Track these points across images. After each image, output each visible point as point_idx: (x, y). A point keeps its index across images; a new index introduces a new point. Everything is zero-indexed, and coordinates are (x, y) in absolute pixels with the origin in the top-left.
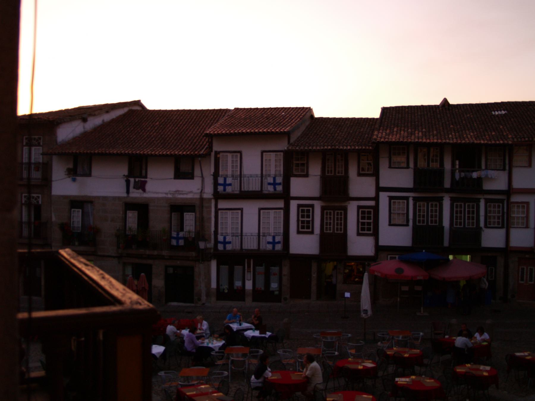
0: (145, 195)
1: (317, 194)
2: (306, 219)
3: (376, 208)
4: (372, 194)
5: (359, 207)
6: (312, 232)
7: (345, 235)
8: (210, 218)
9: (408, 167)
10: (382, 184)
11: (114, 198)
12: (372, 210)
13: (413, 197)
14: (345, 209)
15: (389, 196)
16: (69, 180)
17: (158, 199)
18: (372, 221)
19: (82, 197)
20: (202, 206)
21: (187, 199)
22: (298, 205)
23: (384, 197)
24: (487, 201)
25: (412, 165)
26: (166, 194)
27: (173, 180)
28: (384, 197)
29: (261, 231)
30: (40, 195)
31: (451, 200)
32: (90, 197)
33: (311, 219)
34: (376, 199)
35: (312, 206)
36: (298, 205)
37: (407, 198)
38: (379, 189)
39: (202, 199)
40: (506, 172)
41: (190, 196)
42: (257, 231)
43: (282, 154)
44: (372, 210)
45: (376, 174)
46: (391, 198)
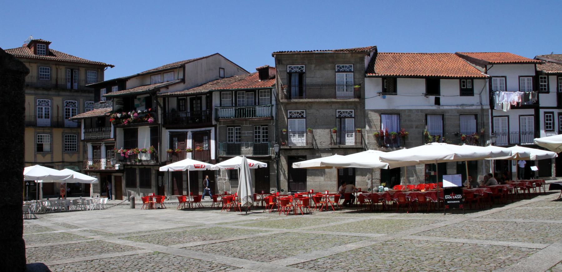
0: (441, 108)
1: (555, 105)
2: (549, 122)
8: (489, 123)
11: (417, 111)
16: (379, 99)
17: (452, 110)
19: (391, 110)
20: (482, 115)
21: (472, 110)
22: (544, 112)
26: (457, 106)
27: (459, 96)
29: (521, 131)
30: (353, 110)
32: (397, 110)
35: (553, 113)
36: (544, 112)
39: (482, 110)
41: (474, 107)
42: (519, 131)
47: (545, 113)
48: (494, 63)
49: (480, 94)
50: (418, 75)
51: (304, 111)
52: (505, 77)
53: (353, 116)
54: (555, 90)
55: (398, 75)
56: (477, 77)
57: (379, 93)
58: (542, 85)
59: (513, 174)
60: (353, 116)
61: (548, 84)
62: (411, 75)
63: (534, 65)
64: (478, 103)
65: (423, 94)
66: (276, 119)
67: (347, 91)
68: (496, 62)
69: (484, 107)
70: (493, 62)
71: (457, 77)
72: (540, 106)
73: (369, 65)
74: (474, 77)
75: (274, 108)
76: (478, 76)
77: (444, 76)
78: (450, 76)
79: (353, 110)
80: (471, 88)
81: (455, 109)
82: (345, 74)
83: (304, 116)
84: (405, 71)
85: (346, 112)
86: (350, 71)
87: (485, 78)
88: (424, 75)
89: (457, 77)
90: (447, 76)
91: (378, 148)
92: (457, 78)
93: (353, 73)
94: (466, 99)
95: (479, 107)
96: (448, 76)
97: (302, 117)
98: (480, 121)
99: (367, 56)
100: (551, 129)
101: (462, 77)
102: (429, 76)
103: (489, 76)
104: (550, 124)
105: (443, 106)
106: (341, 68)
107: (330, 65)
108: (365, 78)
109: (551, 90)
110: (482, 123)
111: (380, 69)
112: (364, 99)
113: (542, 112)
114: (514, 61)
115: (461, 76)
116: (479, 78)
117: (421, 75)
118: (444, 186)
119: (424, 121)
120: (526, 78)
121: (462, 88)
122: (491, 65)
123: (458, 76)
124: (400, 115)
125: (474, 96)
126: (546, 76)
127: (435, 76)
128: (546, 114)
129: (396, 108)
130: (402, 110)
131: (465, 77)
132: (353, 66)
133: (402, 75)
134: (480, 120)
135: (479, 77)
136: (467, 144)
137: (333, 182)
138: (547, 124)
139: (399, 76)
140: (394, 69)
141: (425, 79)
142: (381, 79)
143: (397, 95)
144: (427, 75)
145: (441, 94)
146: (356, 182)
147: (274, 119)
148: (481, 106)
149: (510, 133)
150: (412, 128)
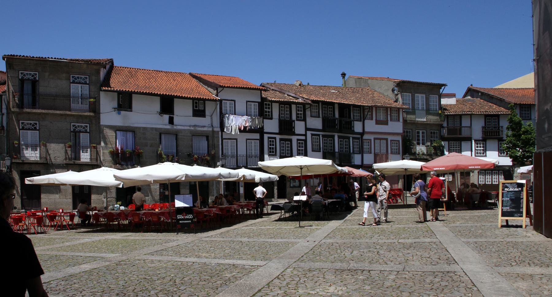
0: (175, 127)
1: (277, 131)
2: (272, 147)
3: (305, 141)
5: (298, 140)
8: (219, 145)
9: (319, 117)
10: (308, 127)
11: (152, 129)
12: (303, 142)
13: (322, 135)
14: (291, 140)
15: (311, 134)
16: (115, 114)
17: (184, 130)
19: (126, 127)
21: (204, 131)
24: (353, 138)
25: (321, 116)
26: (190, 126)
27: (192, 117)
28: (309, 133)
29: (248, 154)
30: (88, 125)
31: (338, 137)
34: (305, 135)
35: (275, 138)
37: (319, 135)
38: (307, 129)
39: (213, 131)
40: (362, 122)
41: (205, 129)
42: (246, 154)
43: (257, 104)
44: (303, 142)
45: (305, 120)
47: (269, 138)
48: (225, 86)
49: (211, 116)
50: (153, 93)
51: (37, 122)
52: (234, 101)
53: (88, 131)
54: (278, 117)
55: (133, 91)
56: (208, 99)
57: (115, 109)
58: (266, 112)
59: (241, 195)
60: (88, 131)
61: (272, 111)
62: (146, 92)
63: (260, 91)
64: (209, 125)
65: (157, 112)
66: (7, 129)
67: (82, 104)
68: (226, 86)
69: (215, 129)
70: (224, 85)
71: (190, 97)
72: (265, 131)
73: (105, 78)
74: (206, 98)
75: (5, 117)
76: (210, 98)
77: (178, 95)
78: (183, 96)
79: (88, 125)
80: (203, 109)
81: (187, 129)
82: (80, 85)
83: (38, 128)
84: (141, 87)
85: (81, 126)
86: (86, 83)
87: (215, 100)
88: (159, 93)
89: (190, 97)
90: (181, 96)
91: (113, 166)
92: (190, 98)
93: (88, 85)
94: (199, 121)
95: (210, 129)
96: (182, 96)
97: (35, 129)
98: (211, 143)
99: (103, 68)
100: (274, 154)
101: (195, 97)
102: (163, 94)
103: (219, 99)
104: (273, 148)
105: (176, 125)
106: (76, 79)
107: (64, 75)
108: (101, 92)
109: (274, 117)
110: (213, 144)
111: (116, 83)
112: (99, 113)
113: (266, 136)
114: (243, 87)
115: (194, 97)
116: (211, 100)
117: (156, 93)
118: (176, 206)
119: (158, 140)
120: (253, 104)
121: (195, 108)
122: (222, 88)
123: (191, 97)
124: (135, 132)
125: (205, 117)
126: (270, 103)
127: (169, 95)
128: (269, 140)
129: (132, 125)
130: (137, 128)
131: (198, 98)
132: (88, 78)
133: (137, 91)
134: (211, 141)
135: (211, 99)
136: (198, 165)
137: (68, 200)
138: (270, 148)
139: (135, 93)
140: (130, 85)
141: (159, 97)
142: (116, 94)
143: (132, 111)
144: (162, 93)
145: (175, 114)
146: (92, 201)
147: (5, 129)
148: (211, 128)
149: (238, 156)
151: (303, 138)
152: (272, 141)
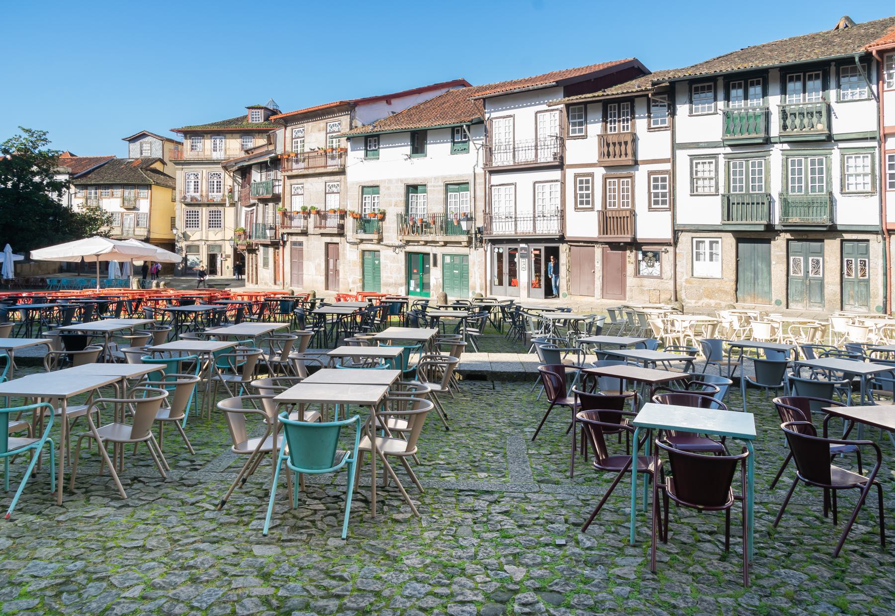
1: (595, 159)
4: (668, 155)
5: (650, 173)
6: (592, 209)
7: (633, 213)
10: (679, 140)
18: (667, 190)
23: (683, 156)
28: (683, 156)
33: (590, 192)
35: (592, 175)
37: (715, 156)
38: (675, 146)
46: (692, 157)
47: (576, 176)
150: (391, 205)
151: (668, 166)
152: (584, 182)
